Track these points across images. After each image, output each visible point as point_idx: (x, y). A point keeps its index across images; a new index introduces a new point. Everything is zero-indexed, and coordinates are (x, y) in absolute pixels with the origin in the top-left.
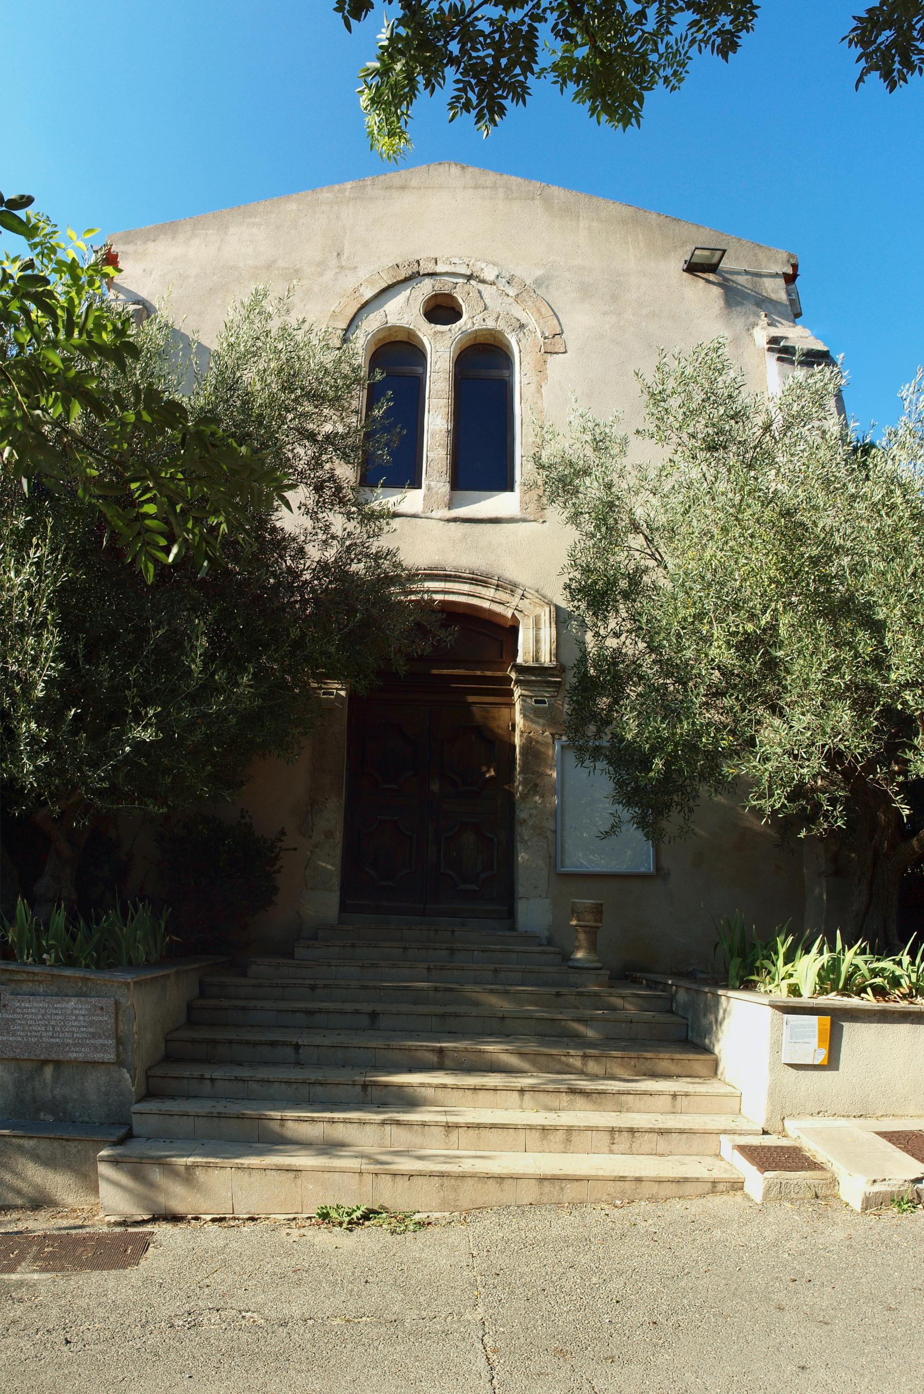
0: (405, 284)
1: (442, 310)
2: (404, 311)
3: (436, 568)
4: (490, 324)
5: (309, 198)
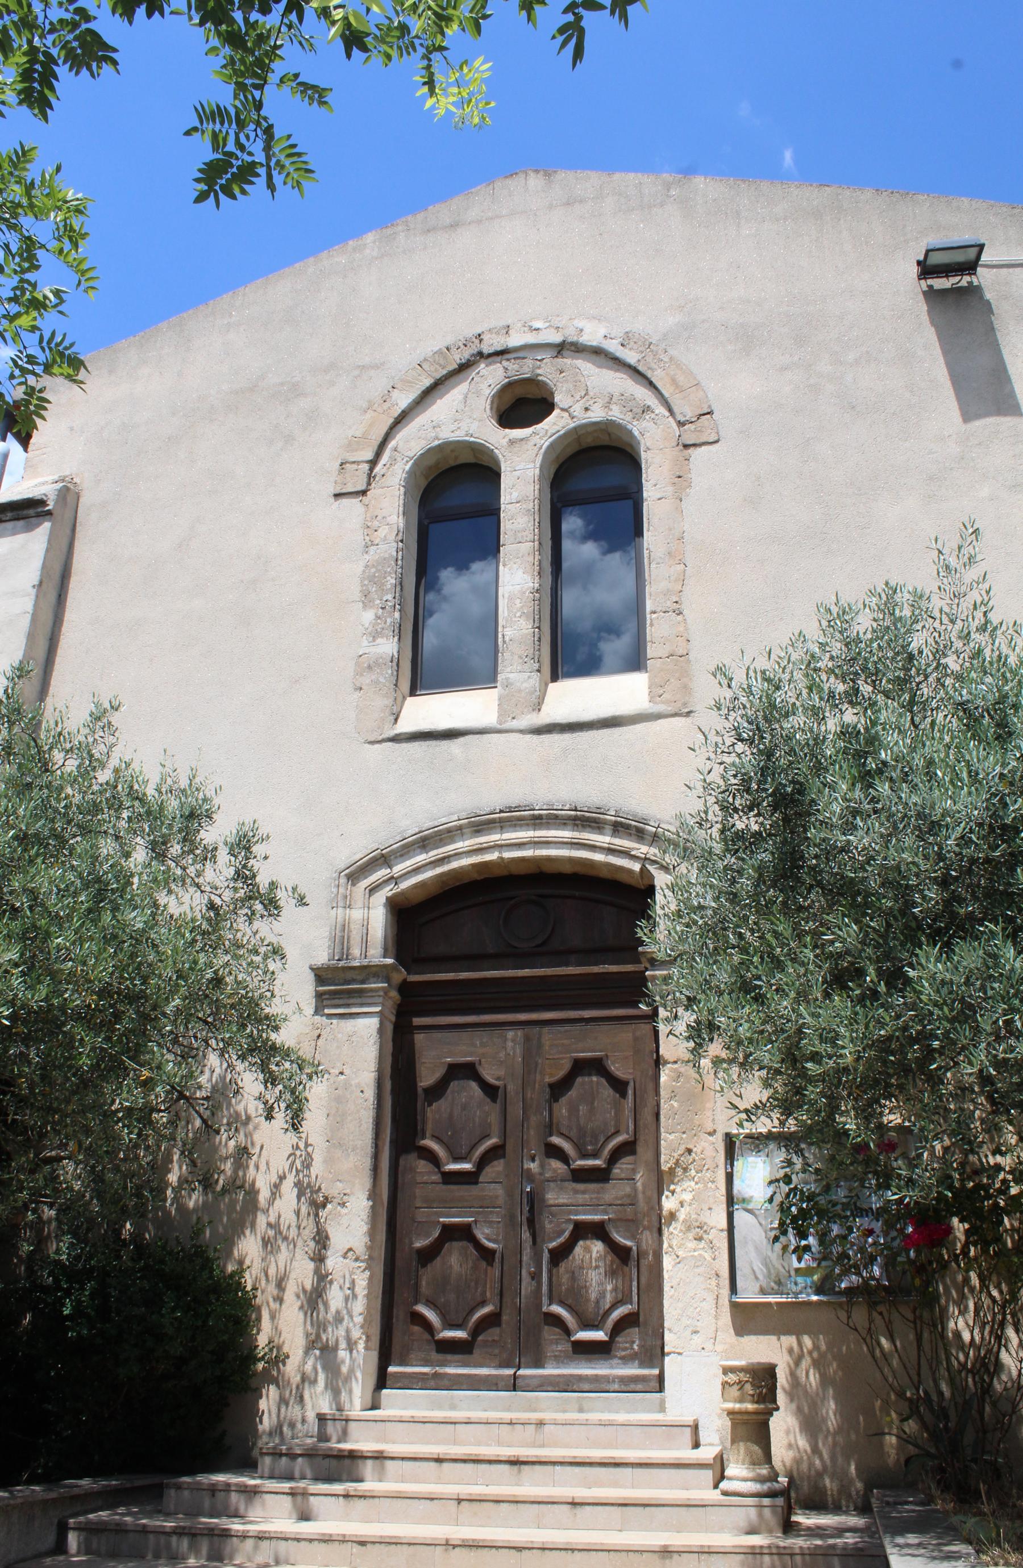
0: (461, 376)
1: (522, 405)
2: (463, 416)
3: (518, 808)
4: (597, 414)
5: (311, 270)
